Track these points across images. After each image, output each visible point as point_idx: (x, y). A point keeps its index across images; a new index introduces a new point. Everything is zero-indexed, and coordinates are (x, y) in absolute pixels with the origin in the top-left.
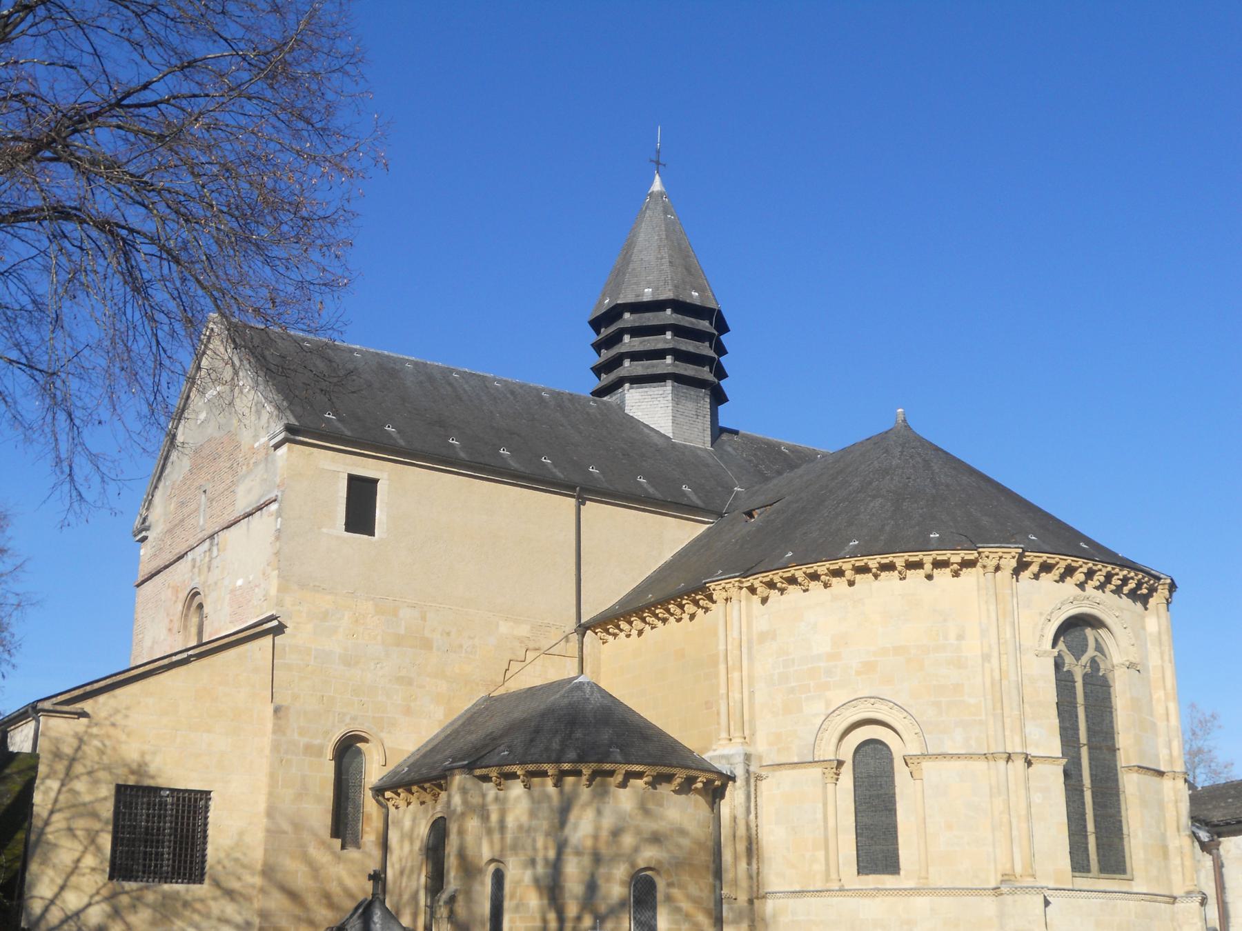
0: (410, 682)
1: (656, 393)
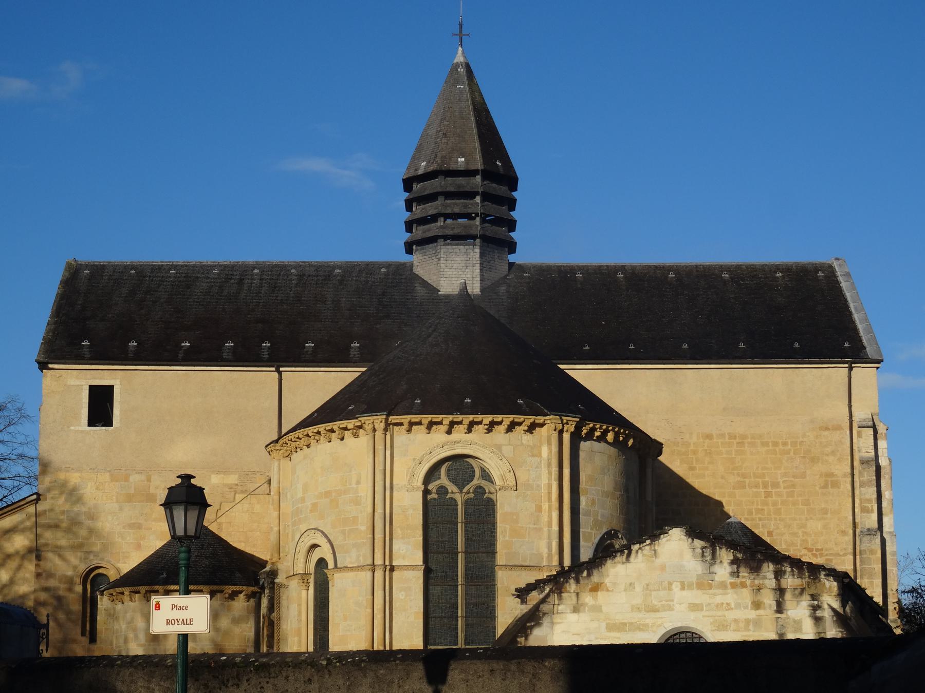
0: (139, 526)
1: (431, 252)
